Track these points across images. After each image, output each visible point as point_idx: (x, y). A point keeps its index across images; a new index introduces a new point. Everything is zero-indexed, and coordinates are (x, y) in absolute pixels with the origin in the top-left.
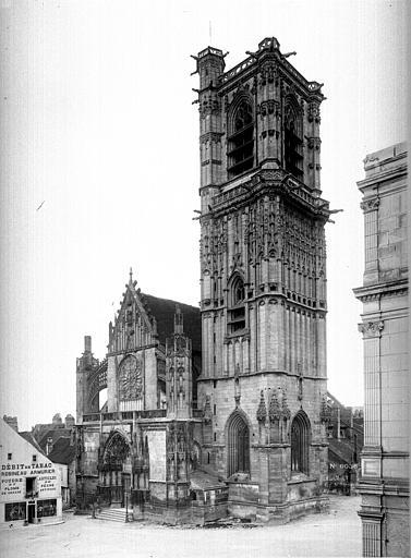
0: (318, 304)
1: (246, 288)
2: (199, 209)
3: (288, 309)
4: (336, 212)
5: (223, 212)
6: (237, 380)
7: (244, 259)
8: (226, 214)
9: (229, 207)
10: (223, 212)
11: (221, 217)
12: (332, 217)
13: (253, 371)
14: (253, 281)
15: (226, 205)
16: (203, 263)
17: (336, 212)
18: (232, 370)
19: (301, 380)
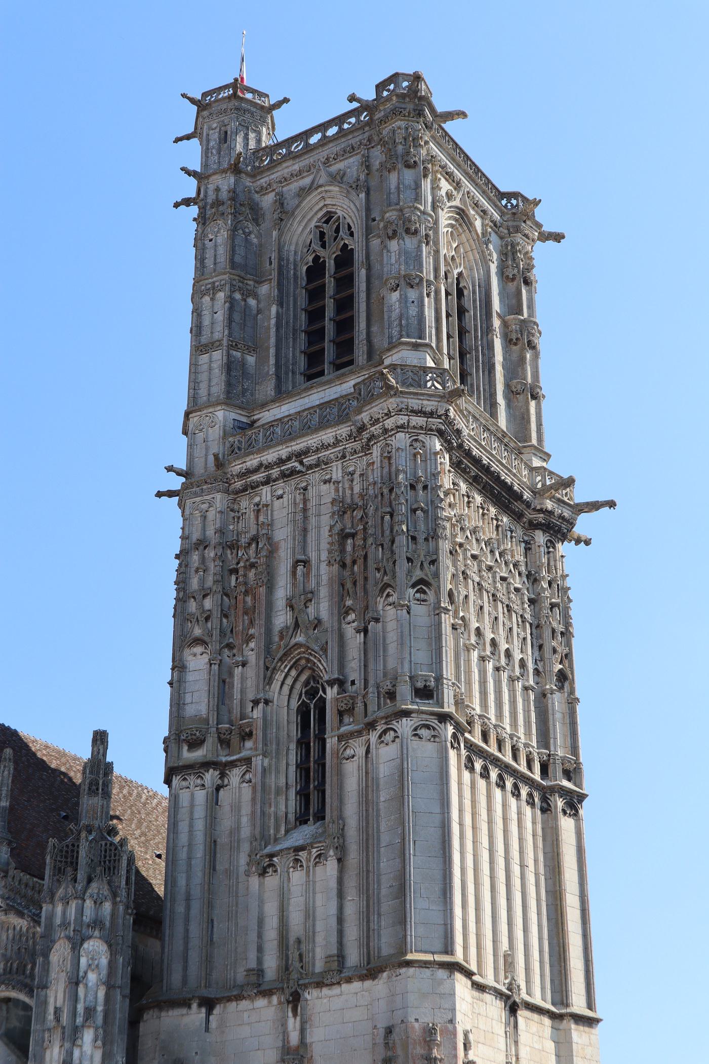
0: (557, 770)
1: (331, 693)
2: (182, 465)
3: (485, 775)
4: (595, 506)
6: (295, 1000)
7: (323, 608)
8: (267, 481)
9: (281, 462)
12: (583, 525)
13: (353, 957)
14: (354, 671)
15: (270, 456)
16: (181, 614)
17: (595, 506)
18: (271, 963)
19: (513, 1009)
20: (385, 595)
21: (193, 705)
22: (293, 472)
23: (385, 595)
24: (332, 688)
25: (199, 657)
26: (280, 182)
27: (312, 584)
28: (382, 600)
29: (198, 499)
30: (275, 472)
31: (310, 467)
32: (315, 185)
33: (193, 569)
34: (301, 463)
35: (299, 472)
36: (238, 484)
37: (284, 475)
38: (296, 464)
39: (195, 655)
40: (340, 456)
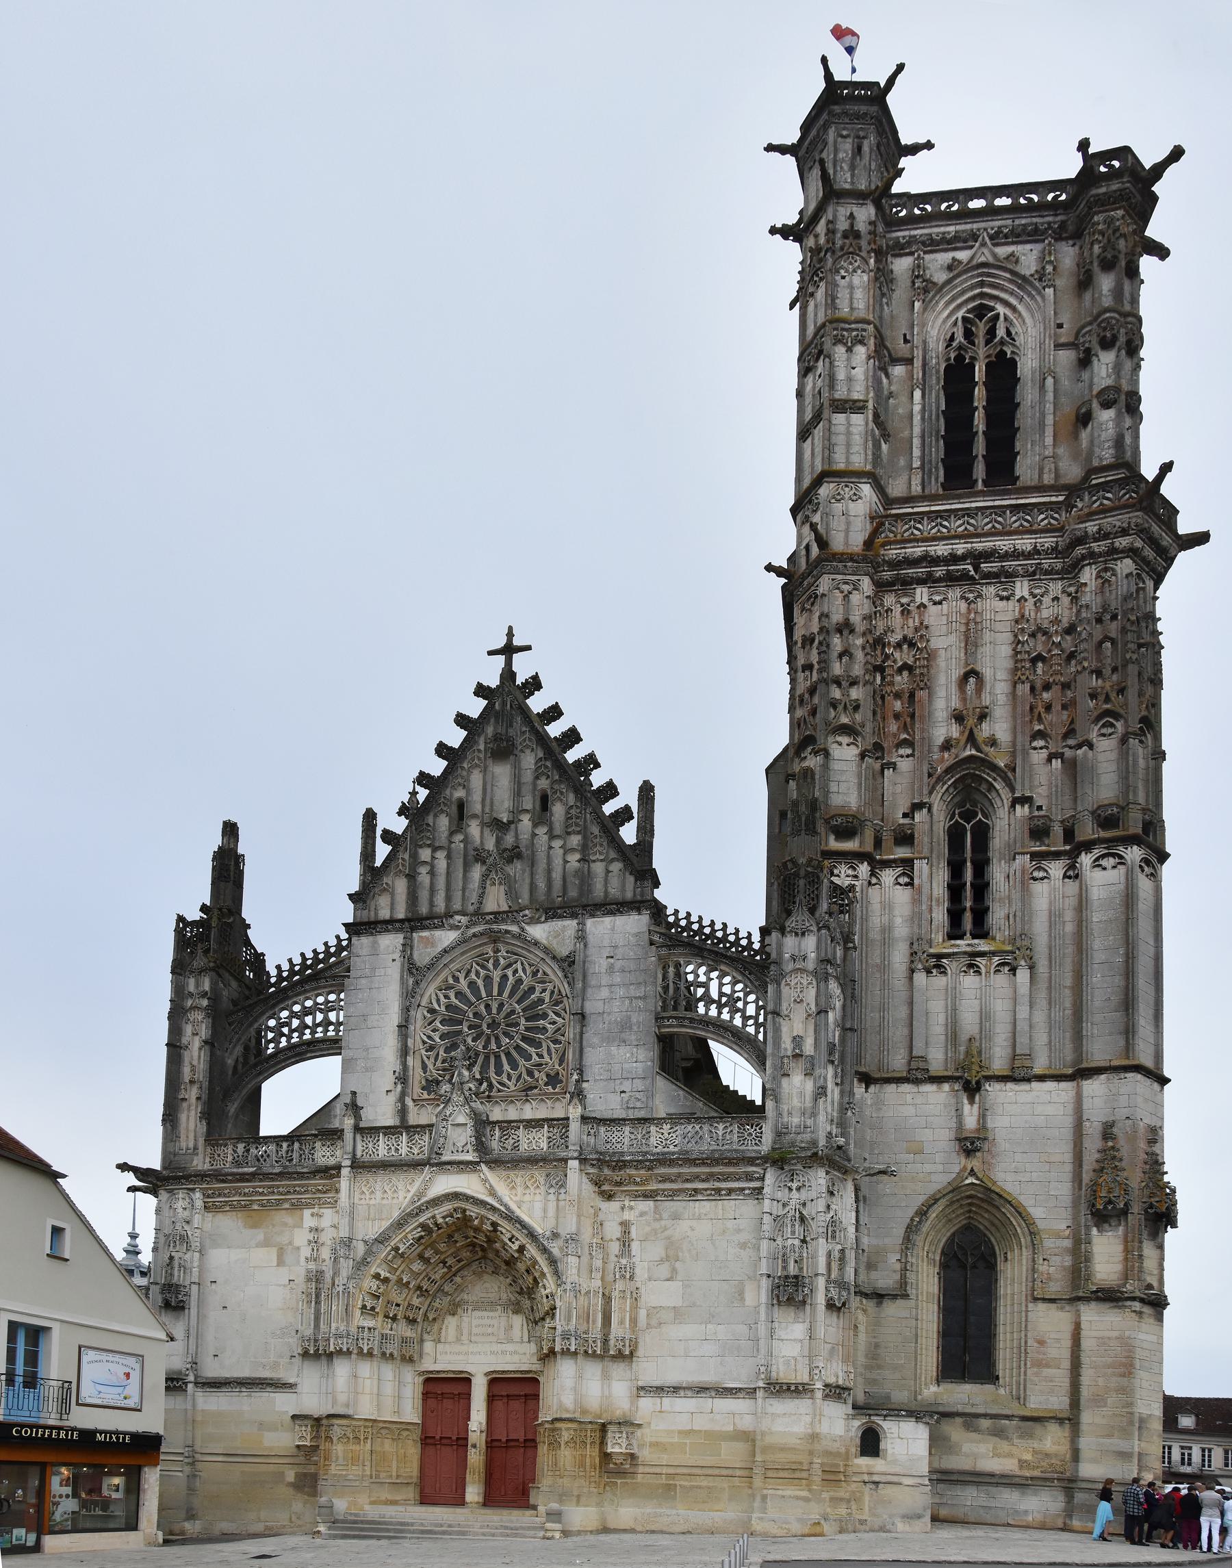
5: (921, 571)
7: (999, 727)
10: (921, 571)
11: (907, 584)
20: (1101, 723)
21: (840, 796)
22: (964, 578)
23: (1101, 723)
24: (1023, 806)
25: (846, 747)
26: (923, 243)
27: (986, 700)
28: (1096, 728)
29: (840, 577)
30: (939, 571)
31: (988, 575)
32: (974, 262)
33: (836, 654)
34: (976, 568)
35: (972, 578)
36: (887, 575)
37: (952, 579)
38: (970, 567)
39: (840, 744)
40: (1031, 570)
